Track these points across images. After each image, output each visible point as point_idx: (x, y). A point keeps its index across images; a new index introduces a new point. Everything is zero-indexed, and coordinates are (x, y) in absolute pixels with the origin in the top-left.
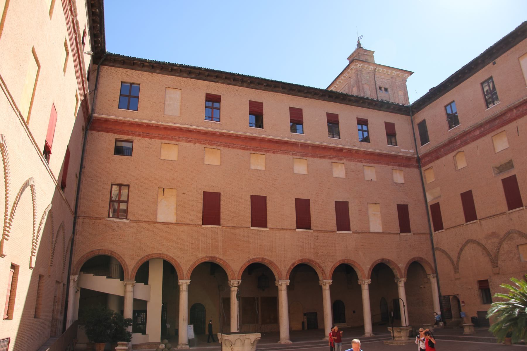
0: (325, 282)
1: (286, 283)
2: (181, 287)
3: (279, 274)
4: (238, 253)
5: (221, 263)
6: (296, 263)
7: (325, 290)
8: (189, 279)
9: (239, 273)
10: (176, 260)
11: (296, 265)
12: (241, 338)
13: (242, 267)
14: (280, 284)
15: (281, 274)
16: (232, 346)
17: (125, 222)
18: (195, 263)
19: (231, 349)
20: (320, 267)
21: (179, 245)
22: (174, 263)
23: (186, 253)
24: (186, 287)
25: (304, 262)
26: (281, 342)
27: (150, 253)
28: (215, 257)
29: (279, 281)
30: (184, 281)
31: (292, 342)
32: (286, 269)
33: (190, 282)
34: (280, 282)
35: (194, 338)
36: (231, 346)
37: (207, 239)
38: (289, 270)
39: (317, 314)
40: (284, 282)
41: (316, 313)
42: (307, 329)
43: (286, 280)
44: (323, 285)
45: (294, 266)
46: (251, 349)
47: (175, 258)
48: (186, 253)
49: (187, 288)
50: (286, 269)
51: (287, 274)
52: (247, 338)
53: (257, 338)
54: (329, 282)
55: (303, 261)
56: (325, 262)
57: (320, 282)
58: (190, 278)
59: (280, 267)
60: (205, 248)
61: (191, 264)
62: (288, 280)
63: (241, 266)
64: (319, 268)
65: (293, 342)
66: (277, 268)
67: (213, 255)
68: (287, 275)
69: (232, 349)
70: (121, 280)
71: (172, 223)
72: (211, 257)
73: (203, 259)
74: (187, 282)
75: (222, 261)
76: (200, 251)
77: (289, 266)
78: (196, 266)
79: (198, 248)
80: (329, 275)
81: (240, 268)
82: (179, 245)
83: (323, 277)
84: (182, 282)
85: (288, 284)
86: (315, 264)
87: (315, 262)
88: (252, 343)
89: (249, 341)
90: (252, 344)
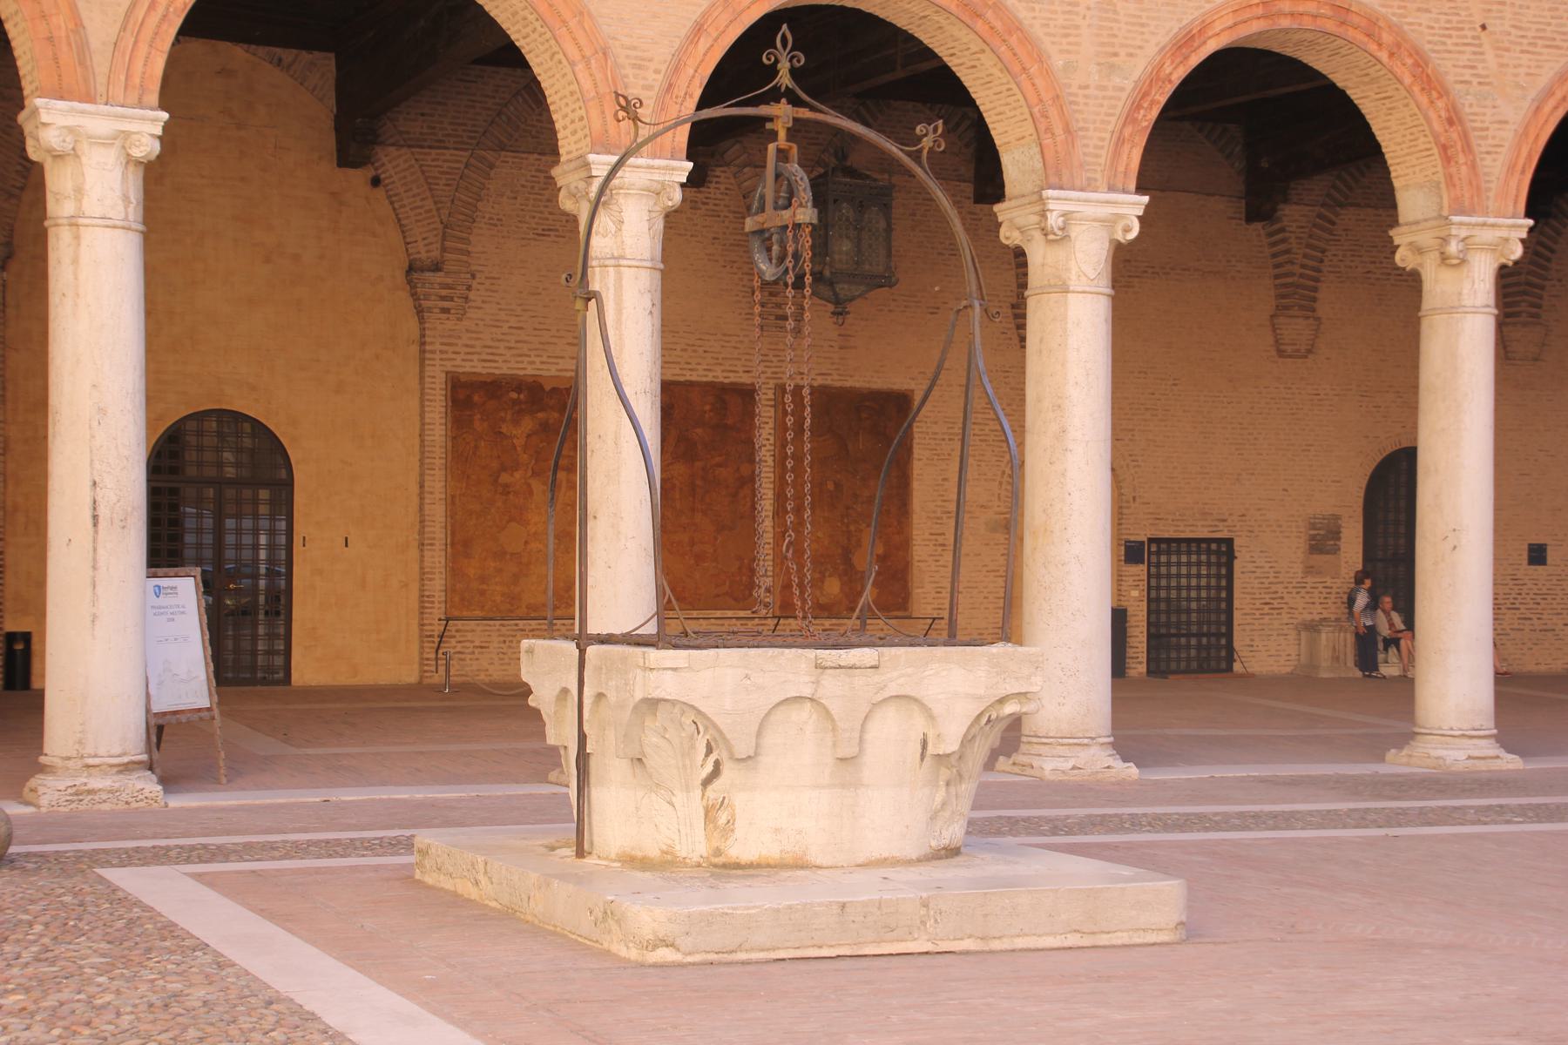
0: (1463, 233)
1: (1110, 222)
2: (58, 182)
3: (1048, 130)
6: (1218, 27)
7: (1452, 310)
8: (154, 98)
11: (1212, 46)
12: (833, 688)
13: (698, 29)
14: (1054, 220)
15: (1067, 130)
16: (717, 784)
19: (709, 813)
20: (1431, 83)
24: (117, 185)
25: (1285, 23)
26: (1036, 762)
29: (1049, 193)
30: (97, 121)
31: (1132, 771)
32: (1117, 81)
34: (1059, 203)
35: (204, 702)
36: (707, 782)
38: (1146, 94)
39: (1230, 556)
40: (1090, 210)
41: (1229, 542)
42: (1143, 668)
43: (1111, 188)
44: (1444, 258)
45: (1195, 60)
46: (934, 817)
49: (126, 198)
50: (1117, 81)
51: (1127, 131)
52: (893, 690)
53: (1002, 701)
54: (1504, 233)
55: (1281, 14)
56: (1483, 35)
57: (1399, 236)
58: (155, 87)
59: (1058, 62)
62: (1125, 191)
64: (1424, 100)
65: (1522, 753)
66: (1034, 70)
68: (1120, 142)
69: (723, 818)
74: (126, 135)
77: (1151, 50)
80: (1511, 169)
81: (683, 32)
83: (1450, 179)
84: (70, 130)
85: (1127, 230)
86: (1384, 56)
87: (1386, 38)
88: (944, 749)
89: (919, 725)
90: (940, 758)
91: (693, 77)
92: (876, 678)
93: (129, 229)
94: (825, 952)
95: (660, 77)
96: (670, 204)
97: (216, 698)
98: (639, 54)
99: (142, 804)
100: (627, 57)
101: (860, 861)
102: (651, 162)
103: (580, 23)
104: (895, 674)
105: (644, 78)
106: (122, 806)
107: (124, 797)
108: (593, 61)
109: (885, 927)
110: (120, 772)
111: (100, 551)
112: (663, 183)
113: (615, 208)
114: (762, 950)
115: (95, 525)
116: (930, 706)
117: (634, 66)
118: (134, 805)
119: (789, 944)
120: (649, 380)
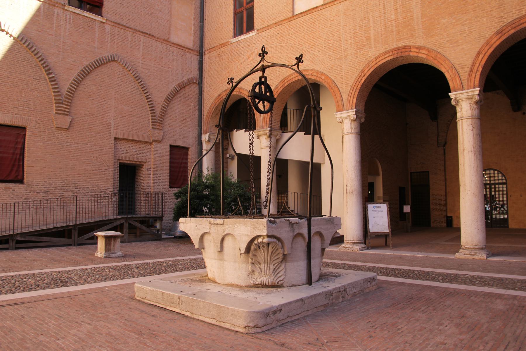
4: (466, 20)
5: (423, 57)
9: (471, 70)
10: (328, 74)
13: (479, 53)
17: (252, 36)
18: (363, 71)
21: (331, 45)
22: (325, 81)
23: (345, 57)
27: (287, 75)
28: (405, 47)
33: (354, 113)
35: (388, 231)
37: (385, 13)
47: (325, 72)
48: (345, 57)
60: (383, 33)
61: (356, 75)
63: (477, 50)
67: (401, 44)
70: (245, 131)
71: (317, 7)
72: (397, 49)
73: (381, 58)
74: (349, 116)
75: (424, 52)
76: (373, 43)
78: (366, 77)
79: (368, 38)
81: (475, 55)
82: (331, 45)
84: (340, 117)
91: (479, 66)
92: (223, 228)
93: (352, 134)
94: (160, 305)
95: (468, 69)
96: (475, 100)
97: (390, 230)
98: (463, 65)
99: (355, 251)
100: (459, 67)
101: (226, 283)
102: (467, 91)
103: (445, 63)
104: (227, 227)
105: (465, 70)
106: (351, 251)
107: (352, 249)
108: (449, 71)
109: (171, 302)
110: (353, 244)
111: (348, 199)
112: (472, 95)
113: (460, 105)
114: (149, 300)
115: (347, 194)
116: (236, 237)
117: (461, 68)
118: (354, 251)
119: (153, 300)
120: (473, 148)
